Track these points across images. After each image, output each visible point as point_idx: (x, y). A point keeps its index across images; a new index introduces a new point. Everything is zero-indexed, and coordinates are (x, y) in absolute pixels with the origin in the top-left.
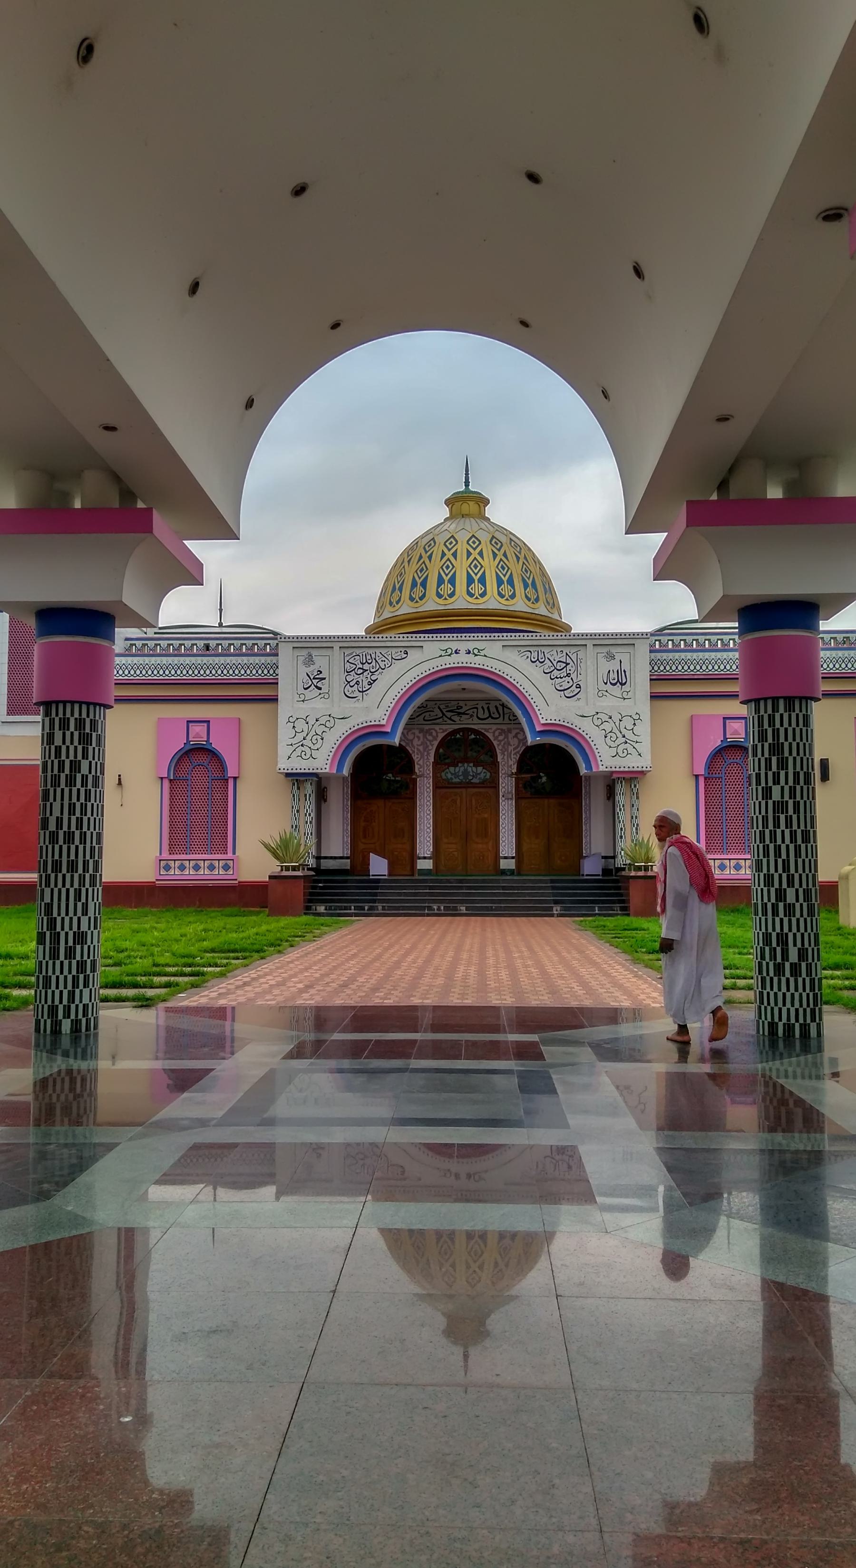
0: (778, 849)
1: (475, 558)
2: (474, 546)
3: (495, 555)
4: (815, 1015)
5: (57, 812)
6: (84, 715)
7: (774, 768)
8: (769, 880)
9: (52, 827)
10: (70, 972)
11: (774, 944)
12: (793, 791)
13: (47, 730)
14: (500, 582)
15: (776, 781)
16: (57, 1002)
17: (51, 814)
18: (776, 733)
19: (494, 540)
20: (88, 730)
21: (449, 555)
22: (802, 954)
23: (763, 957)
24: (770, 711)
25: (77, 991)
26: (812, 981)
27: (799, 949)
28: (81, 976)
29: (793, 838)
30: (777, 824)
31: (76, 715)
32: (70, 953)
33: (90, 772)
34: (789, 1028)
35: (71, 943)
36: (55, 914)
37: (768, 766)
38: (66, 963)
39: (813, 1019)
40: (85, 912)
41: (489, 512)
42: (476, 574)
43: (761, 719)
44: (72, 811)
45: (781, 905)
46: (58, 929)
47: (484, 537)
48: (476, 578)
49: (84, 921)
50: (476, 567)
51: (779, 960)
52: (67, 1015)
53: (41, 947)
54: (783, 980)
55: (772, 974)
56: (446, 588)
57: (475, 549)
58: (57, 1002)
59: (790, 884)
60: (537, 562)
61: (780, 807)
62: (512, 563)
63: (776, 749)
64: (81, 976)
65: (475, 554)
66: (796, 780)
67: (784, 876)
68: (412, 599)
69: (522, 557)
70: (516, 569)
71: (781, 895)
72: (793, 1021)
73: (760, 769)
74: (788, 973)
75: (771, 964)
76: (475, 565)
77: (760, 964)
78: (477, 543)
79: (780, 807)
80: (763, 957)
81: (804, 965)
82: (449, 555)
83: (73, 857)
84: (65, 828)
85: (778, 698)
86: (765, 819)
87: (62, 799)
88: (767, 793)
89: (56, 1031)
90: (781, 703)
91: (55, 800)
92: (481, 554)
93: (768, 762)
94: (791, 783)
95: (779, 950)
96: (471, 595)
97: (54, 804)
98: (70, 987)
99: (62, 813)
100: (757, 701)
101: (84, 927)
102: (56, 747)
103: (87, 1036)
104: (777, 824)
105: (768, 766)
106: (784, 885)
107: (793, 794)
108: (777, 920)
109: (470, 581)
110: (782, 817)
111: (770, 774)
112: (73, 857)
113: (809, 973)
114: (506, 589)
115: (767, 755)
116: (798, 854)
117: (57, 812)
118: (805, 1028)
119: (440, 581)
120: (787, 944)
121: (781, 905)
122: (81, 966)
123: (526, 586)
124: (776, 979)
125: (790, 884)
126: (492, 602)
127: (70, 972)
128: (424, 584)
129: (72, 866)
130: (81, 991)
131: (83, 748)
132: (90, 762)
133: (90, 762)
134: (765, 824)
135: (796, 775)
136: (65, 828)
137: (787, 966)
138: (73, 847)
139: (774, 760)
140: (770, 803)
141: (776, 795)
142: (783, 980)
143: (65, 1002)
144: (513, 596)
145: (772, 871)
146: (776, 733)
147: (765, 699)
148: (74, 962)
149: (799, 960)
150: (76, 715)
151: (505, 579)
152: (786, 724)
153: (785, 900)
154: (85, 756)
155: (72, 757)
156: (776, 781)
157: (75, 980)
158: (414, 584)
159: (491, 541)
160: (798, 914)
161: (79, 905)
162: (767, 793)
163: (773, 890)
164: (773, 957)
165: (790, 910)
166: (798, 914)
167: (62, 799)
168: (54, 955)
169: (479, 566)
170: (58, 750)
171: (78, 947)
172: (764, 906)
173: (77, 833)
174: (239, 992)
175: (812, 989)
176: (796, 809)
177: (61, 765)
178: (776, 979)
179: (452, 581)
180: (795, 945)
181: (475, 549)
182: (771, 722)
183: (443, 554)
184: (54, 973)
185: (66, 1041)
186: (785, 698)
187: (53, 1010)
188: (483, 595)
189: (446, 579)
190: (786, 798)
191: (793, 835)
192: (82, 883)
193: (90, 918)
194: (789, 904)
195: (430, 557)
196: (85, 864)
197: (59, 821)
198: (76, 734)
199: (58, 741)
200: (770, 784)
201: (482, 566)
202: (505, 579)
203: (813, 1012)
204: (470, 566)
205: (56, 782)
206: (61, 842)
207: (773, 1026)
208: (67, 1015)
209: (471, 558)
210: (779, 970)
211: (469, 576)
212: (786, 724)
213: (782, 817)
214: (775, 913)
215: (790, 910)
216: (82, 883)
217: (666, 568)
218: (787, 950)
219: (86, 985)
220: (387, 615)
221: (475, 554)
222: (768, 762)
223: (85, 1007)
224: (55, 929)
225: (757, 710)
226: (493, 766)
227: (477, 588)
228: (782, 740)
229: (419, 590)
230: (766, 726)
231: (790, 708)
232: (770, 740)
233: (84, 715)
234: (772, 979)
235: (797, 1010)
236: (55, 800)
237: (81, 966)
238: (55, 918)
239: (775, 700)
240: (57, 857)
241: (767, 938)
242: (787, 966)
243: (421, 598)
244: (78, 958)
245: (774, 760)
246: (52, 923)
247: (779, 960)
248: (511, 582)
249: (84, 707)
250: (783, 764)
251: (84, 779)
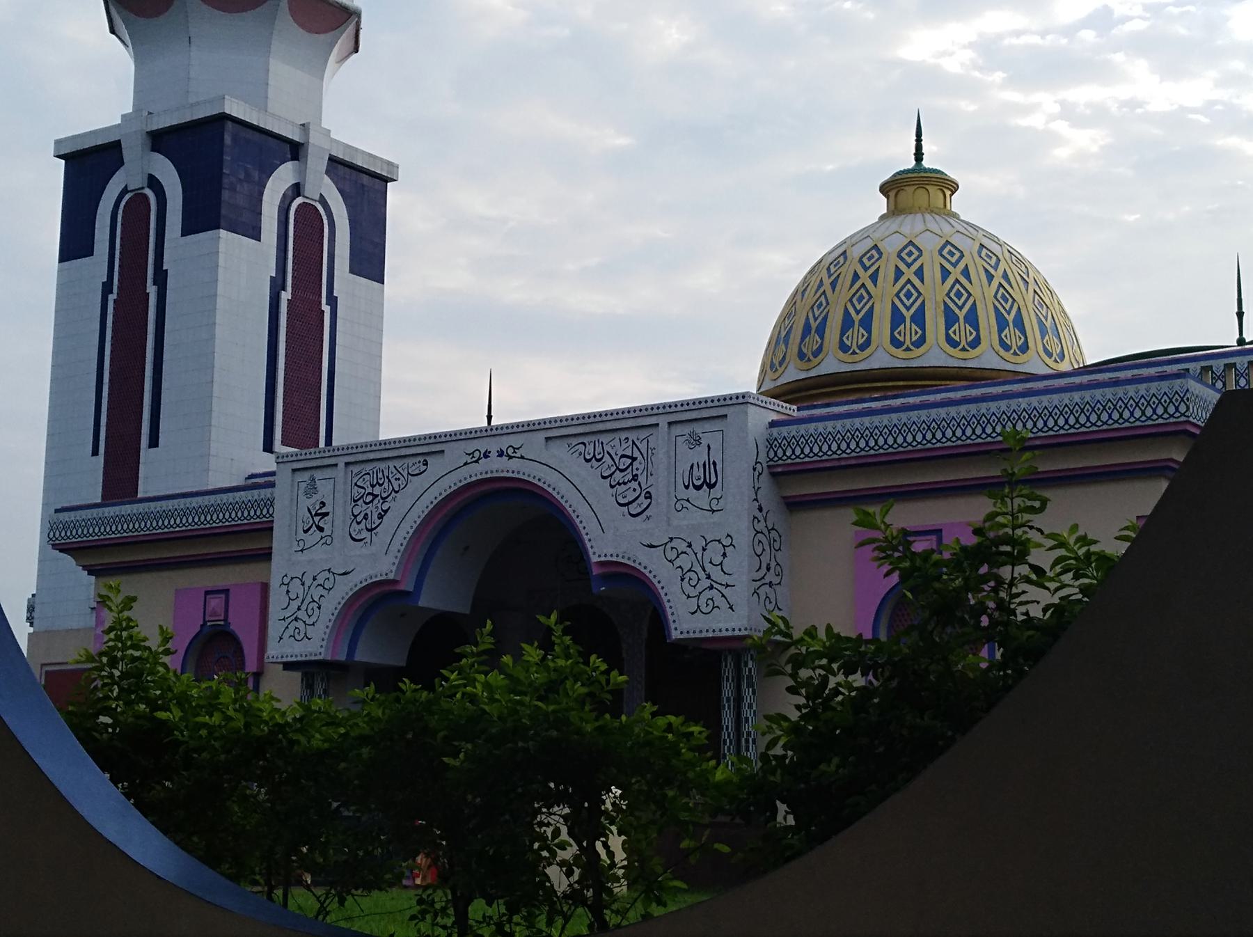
1: (957, 281)
2: (953, 260)
19: (984, 251)
41: (957, 203)
42: (960, 308)
47: (929, 244)
57: (909, 265)
70: (983, 293)
78: (958, 255)
82: (865, 277)
96: (953, 343)
126: (935, 354)
159: (979, 253)
169: (966, 295)
181: (909, 265)
201: (970, 295)
204: (948, 295)
209: (902, 281)
221: (909, 273)
227: (962, 331)
248: (972, 319)
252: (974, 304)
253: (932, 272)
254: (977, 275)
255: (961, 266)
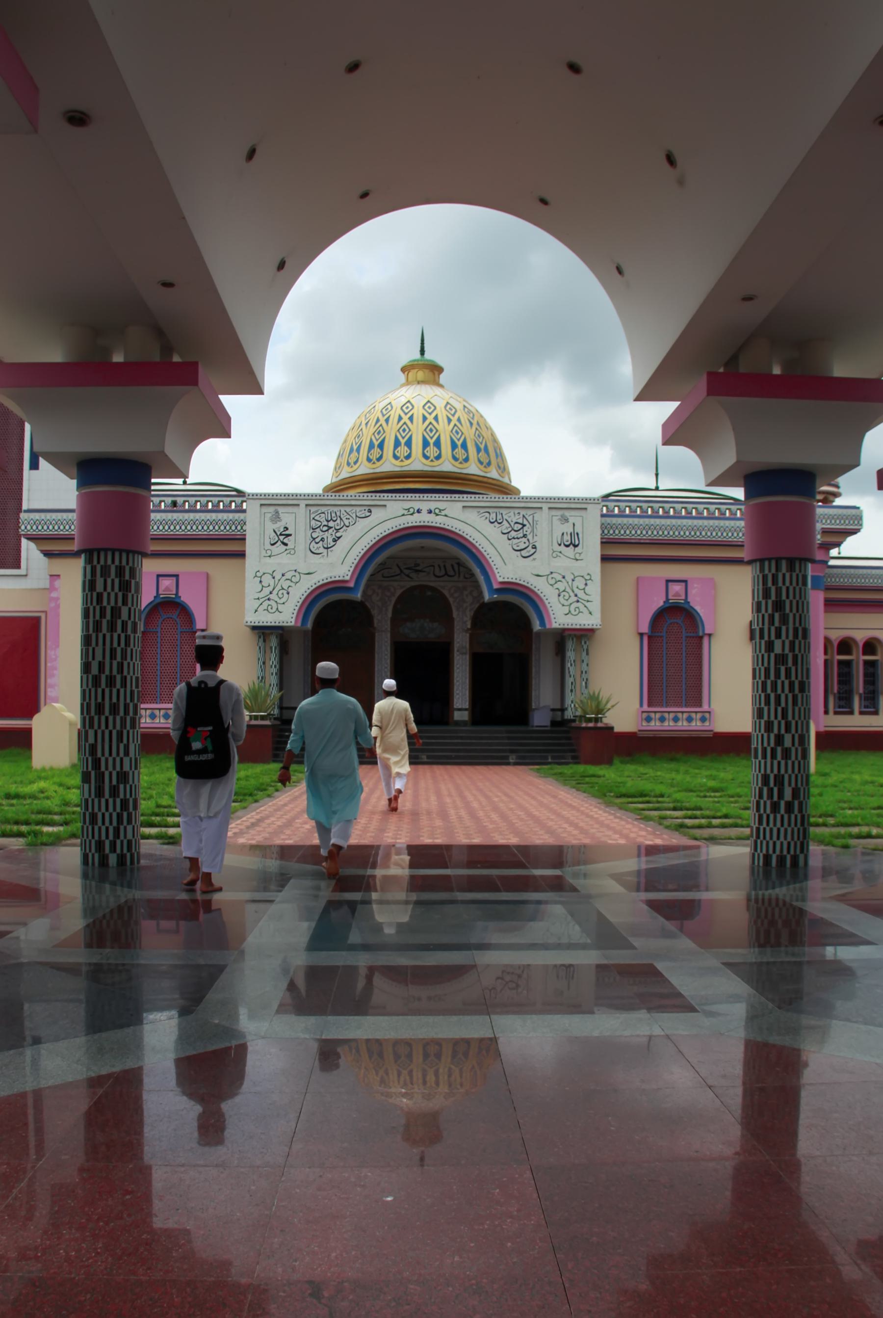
0: (778, 698)
2: (430, 411)
3: (449, 421)
4: (804, 848)
5: (99, 657)
6: (124, 563)
7: (777, 624)
8: (769, 727)
9: (95, 670)
10: (115, 809)
11: (772, 784)
12: (792, 644)
13: (89, 577)
14: (454, 446)
15: (778, 635)
16: (103, 837)
17: (93, 659)
18: (778, 591)
19: (449, 406)
20: (127, 577)
21: (405, 419)
22: (795, 793)
23: (761, 796)
24: (773, 570)
25: (122, 828)
26: (803, 817)
27: (793, 789)
28: (125, 814)
29: (791, 689)
30: (778, 676)
31: (117, 562)
32: (114, 792)
33: (130, 618)
34: (781, 859)
35: (114, 782)
36: (99, 754)
37: (772, 622)
38: (111, 801)
39: (802, 851)
40: (127, 753)
42: (432, 438)
43: (765, 578)
44: (113, 656)
45: (779, 749)
46: (103, 768)
47: (440, 404)
48: (432, 442)
49: (126, 761)
50: (431, 430)
51: (775, 798)
52: (113, 849)
53: (86, 786)
54: (779, 817)
55: (768, 811)
56: (403, 451)
57: (430, 414)
58: (103, 837)
59: (788, 730)
60: (488, 428)
61: (781, 659)
62: (465, 428)
63: (778, 606)
64: (125, 814)
65: (430, 418)
66: (796, 635)
67: (783, 722)
68: (369, 460)
69: (475, 422)
70: (469, 433)
71: (779, 740)
72: (785, 852)
73: (763, 624)
74: (782, 811)
75: (768, 803)
76: (431, 428)
77: (758, 803)
78: (433, 408)
79: (781, 659)
80: (761, 796)
81: (796, 803)
82: (405, 419)
83: (114, 700)
84: (107, 672)
85: (781, 559)
86: (767, 670)
87: (104, 644)
88: (770, 646)
89: (104, 862)
90: (784, 564)
91: (97, 645)
92: (436, 418)
93: (772, 617)
94: (791, 637)
95: (776, 790)
96: (426, 457)
97: (96, 649)
98: (115, 823)
99: (104, 657)
100: (762, 561)
101: (126, 768)
102: (98, 594)
103: (132, 870)
104: (778, 676)
105: (772, 622)
106: (783, 731)
107: (792, 649)
108: (775, 763)
109: (426, 444)
110: (783, 669)
111: (773, 629)
112: (114, 700)
113: (800, 811)
114: (460, 452)
115: (770, 611)
116: (795, 703)
117: (99, 657)
118: (795, 859)
119: (397, 444)
120: (783, 785)
121: (779, 749)
122: (125, 804)
123: (479, 450)
124: (772, 817)
125: (788, 730)
127: (115, 809)
128: (381, 446)
129: (114, 709)
130: (125, 828)
131: (123, 595)
132: (130, 609)
133: (130, 609)
134: (767, 675)
135: (796, 630)
136: (107, 672)
137: (782, 804)
138: (115, 691)
139: (777, 615)
140: (772, 655)
141: (778, 649)
142: (779, 817)
143: (111, 837)
144: (466, 460)
145: (772, 718)
146: (778, 591)
147: (770, 560)
148: (118, 801)
149: (793, 798)
150: (117, 562)
151: (459, 443)
152: (787, 583)
153: (783, 745)
154: (125, 603)
155: (113, 603)
156: (778, 635)
157: (120, 817)
158: (371, 446)
160: (793, 758)
161: (122, 746)
162: (770, 646)
163: (772, 736)
164: (770, 796)
165: (786, 754)
166: (793, 758)
167: (104, 644)
168: (100, 793)
170: (100, 597)
171: (122, 786)
172: (764, 750)
173: (118, 678)
174: (252, 832)
175: (802, 824)
176: (795, 663)
177: (103, 611)
178: (772, 817)
179: (409, 444)
180: (790, 785)
182: (775, 582)
183: (400, 418)
184: (100, 809)
185: (113, 874)
186: (787, 559)
187: (100, 845)
188: (438, 457)
189: (403, 441)
190: (787, 651)
191: (791, 685)
192: (124, 725)
193: (131, 759)
194: (786, 748)
195: (387, 421)
196: (126, 706)
197: (101, 665)
198: (117, 581)
199: (99, 587)
200: (773, 637)
201: (437, 431)
202: (459, 443)
203: (802, 844)
205: (98, 627)
206: (103, 685)
207: (767, 858)
208: (113, 849)
209: (427, 423)
210: (775, 807)
211: (424, 439)
212: (787, 583)
213: (783, 669)
214: (774, 756)
215: (786, 754)
216: (124, 725)
217: (673, 434)
218: (783, 790)
219: (129, 822)
220: (345, 473)
221: (430, 418)
222: (772, 617)
223: (130, 842)
224: (100, 768)
225: (762, 569)
226: (448, 621)
227: (432, 451)
228: (784, 597)
229: (376, 452)
230: (770, 584)
231: (791, 568)
232: (773, 597)
233: (124, 563)
234: (768, 816)
235: (789, 843)
236: (97, 645)
237: (125, 804)
238: (100, 759)
239: (778, 561)
240: (100, 700)
241: (765, 779)
242: (782, 804)
243: (379, 459)
244: (122, 796)
245: (777, 615)
246: (97, 763)
247: (775, 798)
248: (464, 446)
249: (124, 556)
250: (784, 620)
251: (125, 624)
252: (439, 436)
253: (442, 419)
254: (442, 419)
255: (434, 415)
